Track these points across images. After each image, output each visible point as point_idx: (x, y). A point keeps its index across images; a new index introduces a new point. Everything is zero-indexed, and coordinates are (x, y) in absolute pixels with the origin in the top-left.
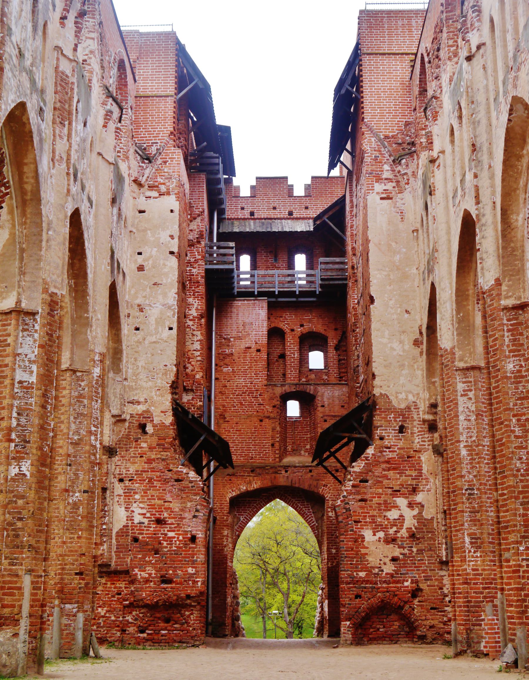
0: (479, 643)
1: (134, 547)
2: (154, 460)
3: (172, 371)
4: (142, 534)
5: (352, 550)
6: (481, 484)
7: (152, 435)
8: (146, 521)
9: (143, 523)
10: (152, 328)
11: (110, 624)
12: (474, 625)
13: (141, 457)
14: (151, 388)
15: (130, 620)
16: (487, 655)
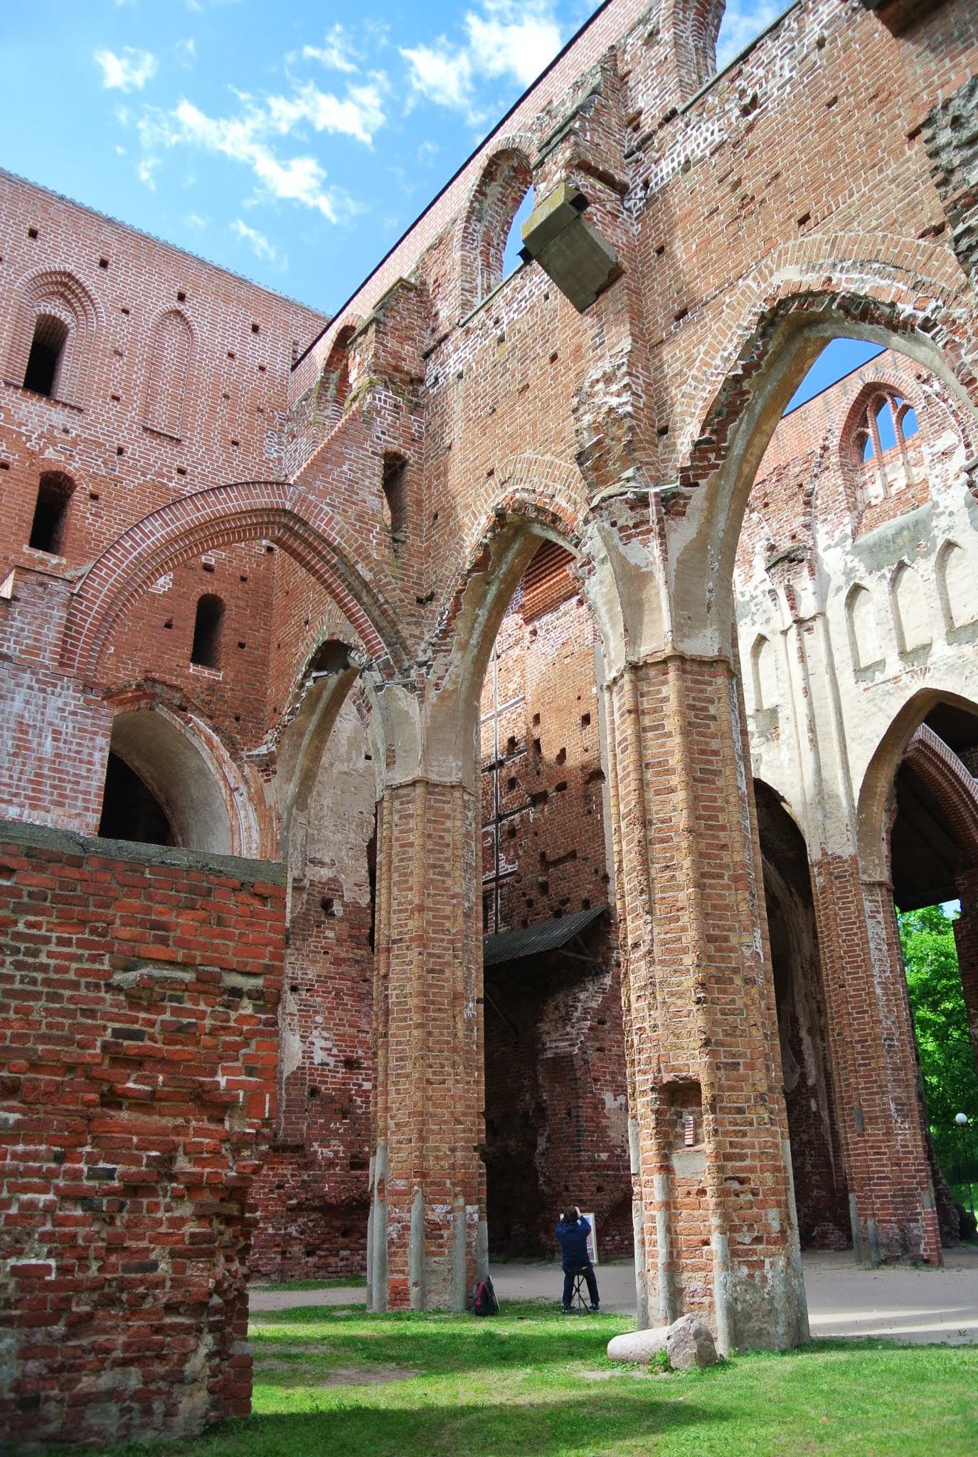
0: (918, 1245)
1: (313, 1105)
2: (344, 960)
3: (370, 823)
4: (326, 1083)
5: (592, 1121)
6: (901, 1034)
7: (342, 920)
8: (331, 1061)
9: (328, 1065)
10: (344, 750)
11: (265, 1241)
12: (909, 1221)
13: (326, 953)
14: (340, 843)
15: (295, 1234)
16: (927, 1262)
